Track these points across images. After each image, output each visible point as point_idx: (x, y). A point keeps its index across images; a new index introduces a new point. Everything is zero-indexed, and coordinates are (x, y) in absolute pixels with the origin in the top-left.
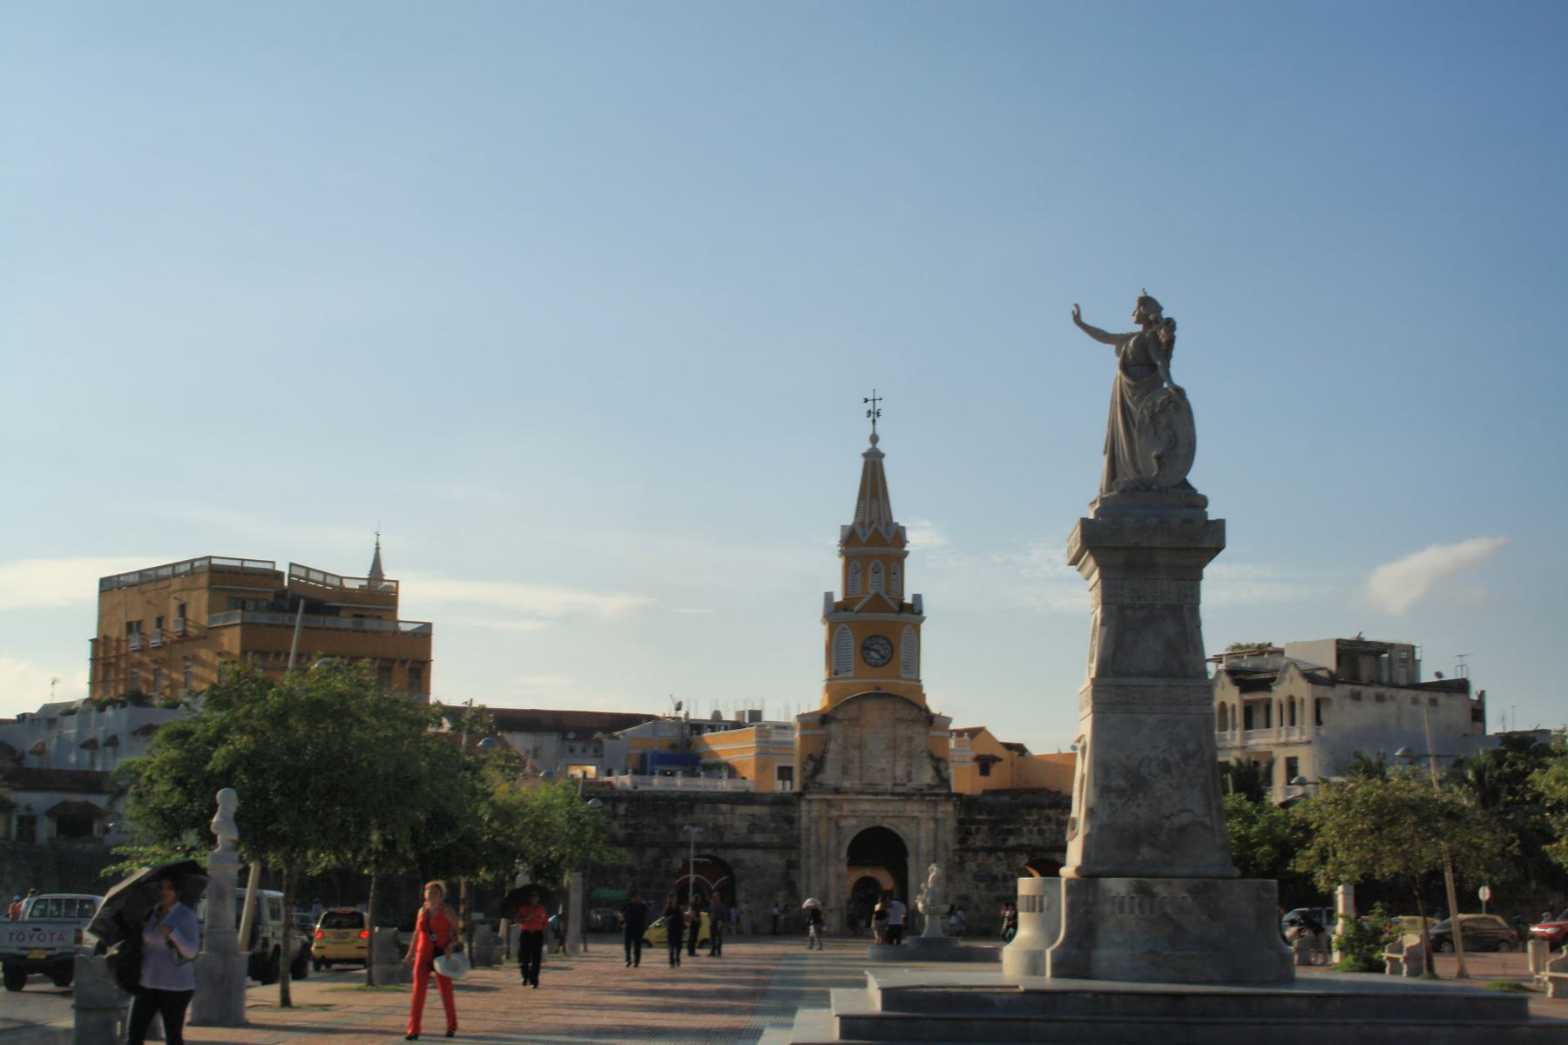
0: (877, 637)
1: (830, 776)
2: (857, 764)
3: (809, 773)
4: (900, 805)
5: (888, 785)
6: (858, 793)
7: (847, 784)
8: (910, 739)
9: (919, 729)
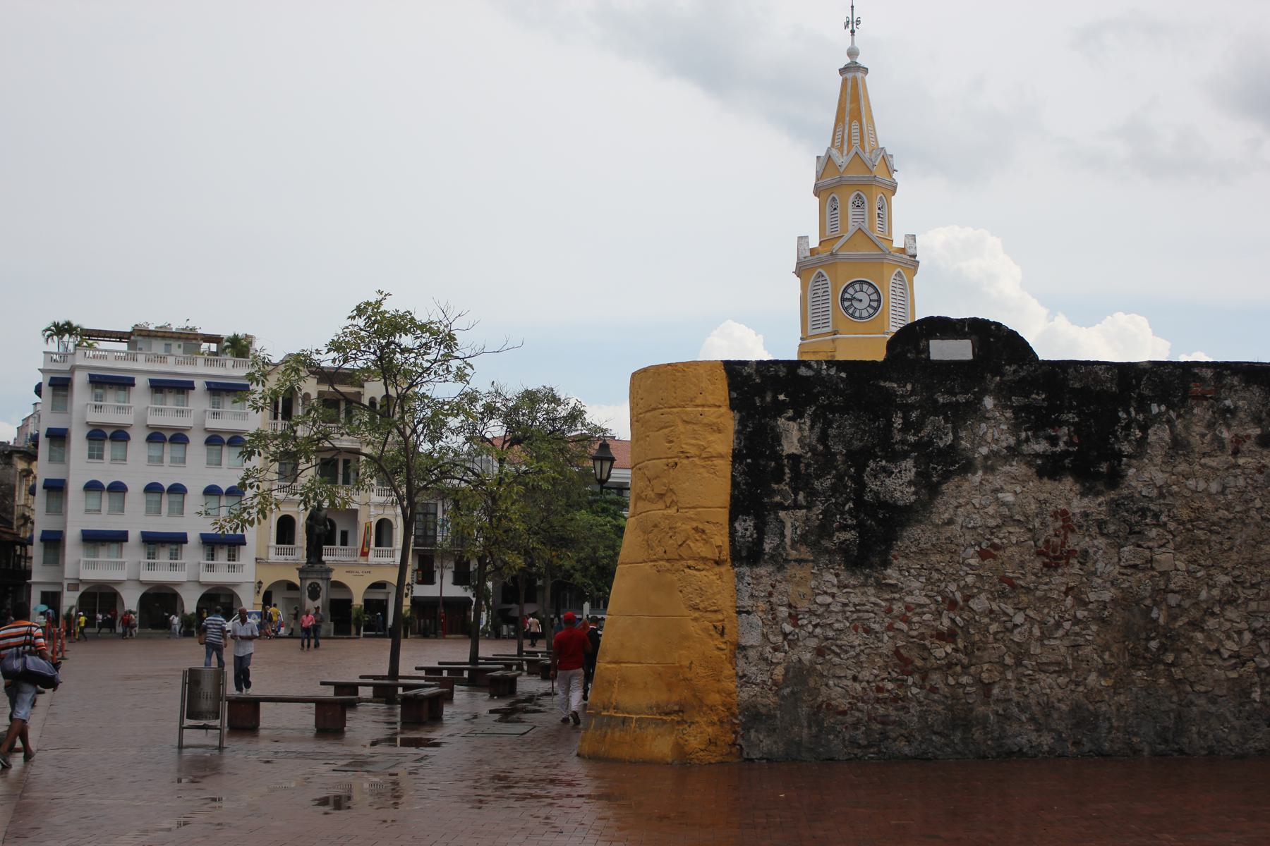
0: (861, 282)
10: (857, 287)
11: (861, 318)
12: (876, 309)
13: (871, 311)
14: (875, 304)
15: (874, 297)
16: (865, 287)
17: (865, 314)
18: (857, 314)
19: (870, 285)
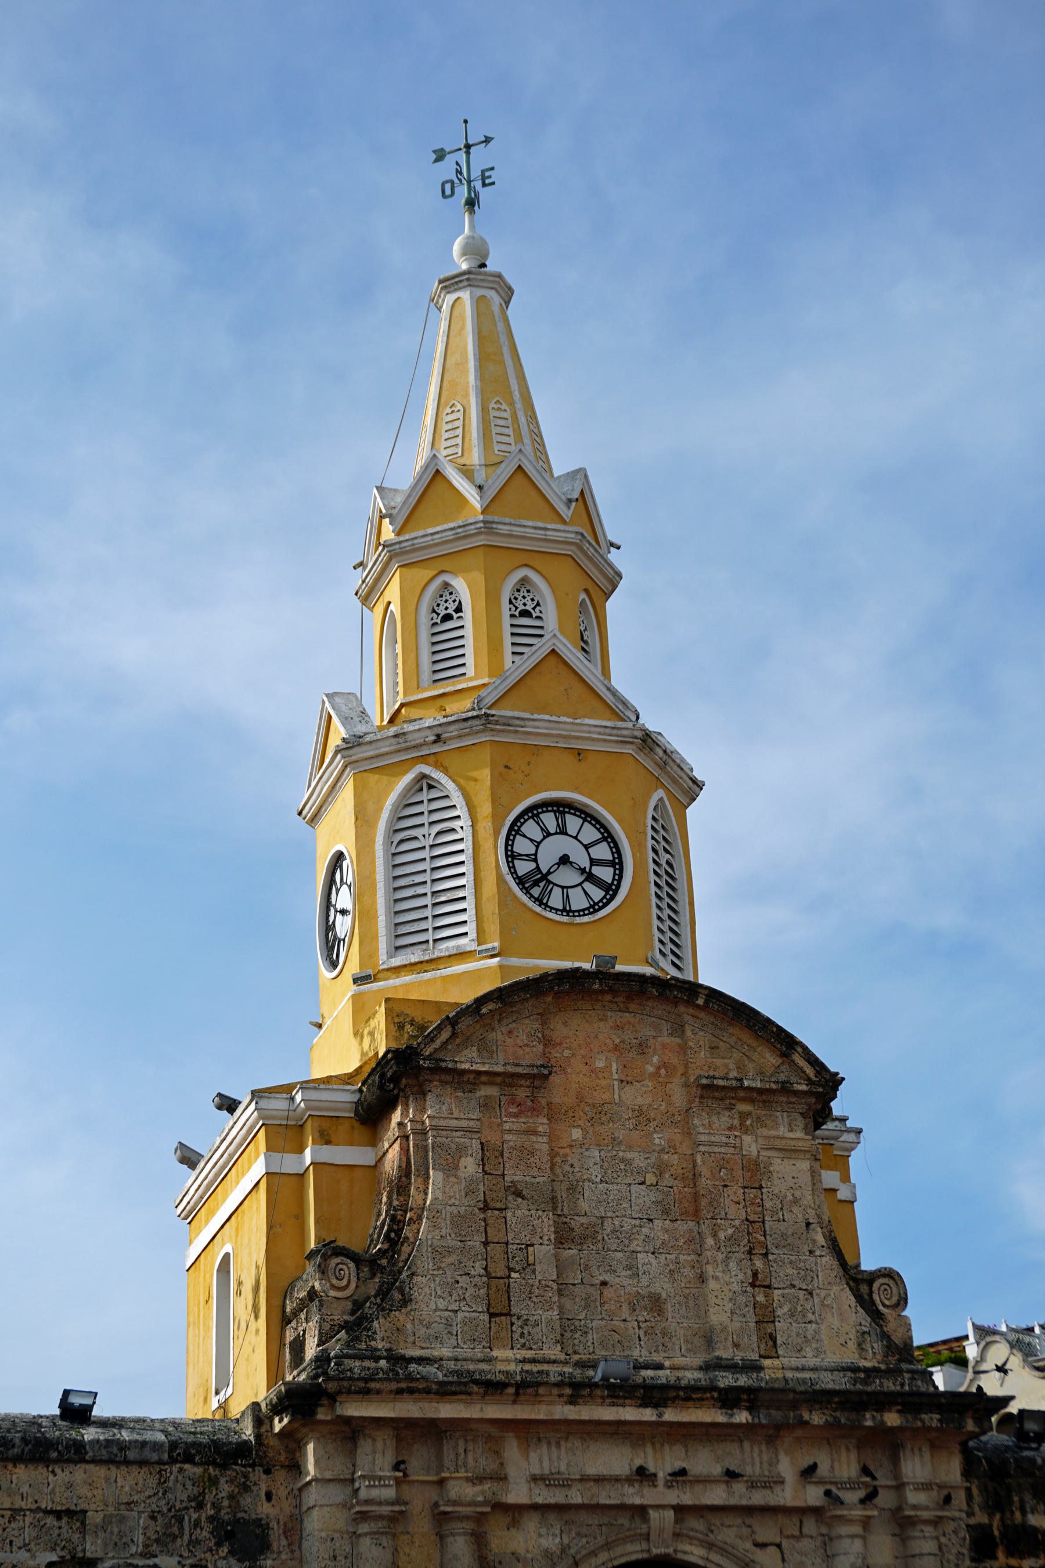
0: (561, 807)
1: (438, 1320)
2: (546, 1271)
3: (340, 1314)
4: (751, 1459)
5: (682, 1364)
6: (578, 1390)
7: (507, 1359)
8: (755, 1175)
9: (787, 1128)
10: (549, 820)
11: (566, 911)
12: (611, 890)
13: (597, 894)
14: (606, 874)
15: (602, 852)
16: (573, 823)
17: (578, 901)
18: (556, 899)
19: (587, 816)
